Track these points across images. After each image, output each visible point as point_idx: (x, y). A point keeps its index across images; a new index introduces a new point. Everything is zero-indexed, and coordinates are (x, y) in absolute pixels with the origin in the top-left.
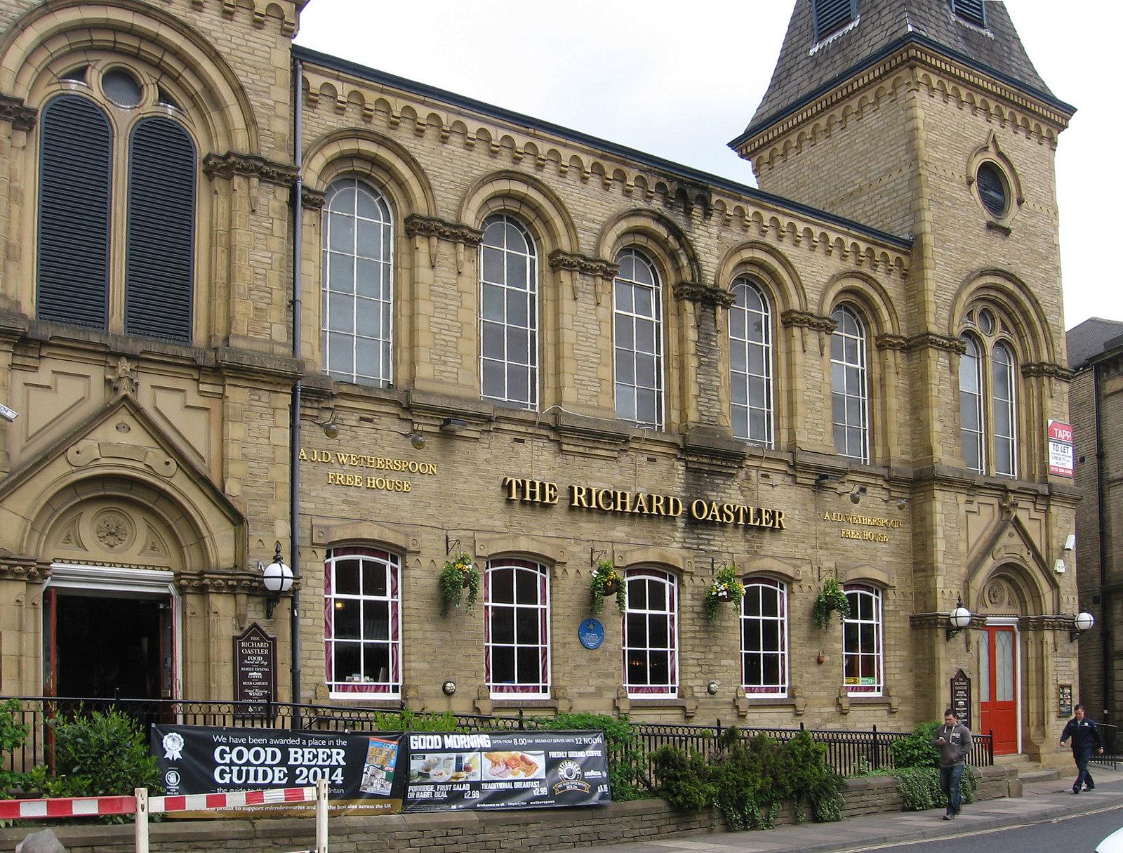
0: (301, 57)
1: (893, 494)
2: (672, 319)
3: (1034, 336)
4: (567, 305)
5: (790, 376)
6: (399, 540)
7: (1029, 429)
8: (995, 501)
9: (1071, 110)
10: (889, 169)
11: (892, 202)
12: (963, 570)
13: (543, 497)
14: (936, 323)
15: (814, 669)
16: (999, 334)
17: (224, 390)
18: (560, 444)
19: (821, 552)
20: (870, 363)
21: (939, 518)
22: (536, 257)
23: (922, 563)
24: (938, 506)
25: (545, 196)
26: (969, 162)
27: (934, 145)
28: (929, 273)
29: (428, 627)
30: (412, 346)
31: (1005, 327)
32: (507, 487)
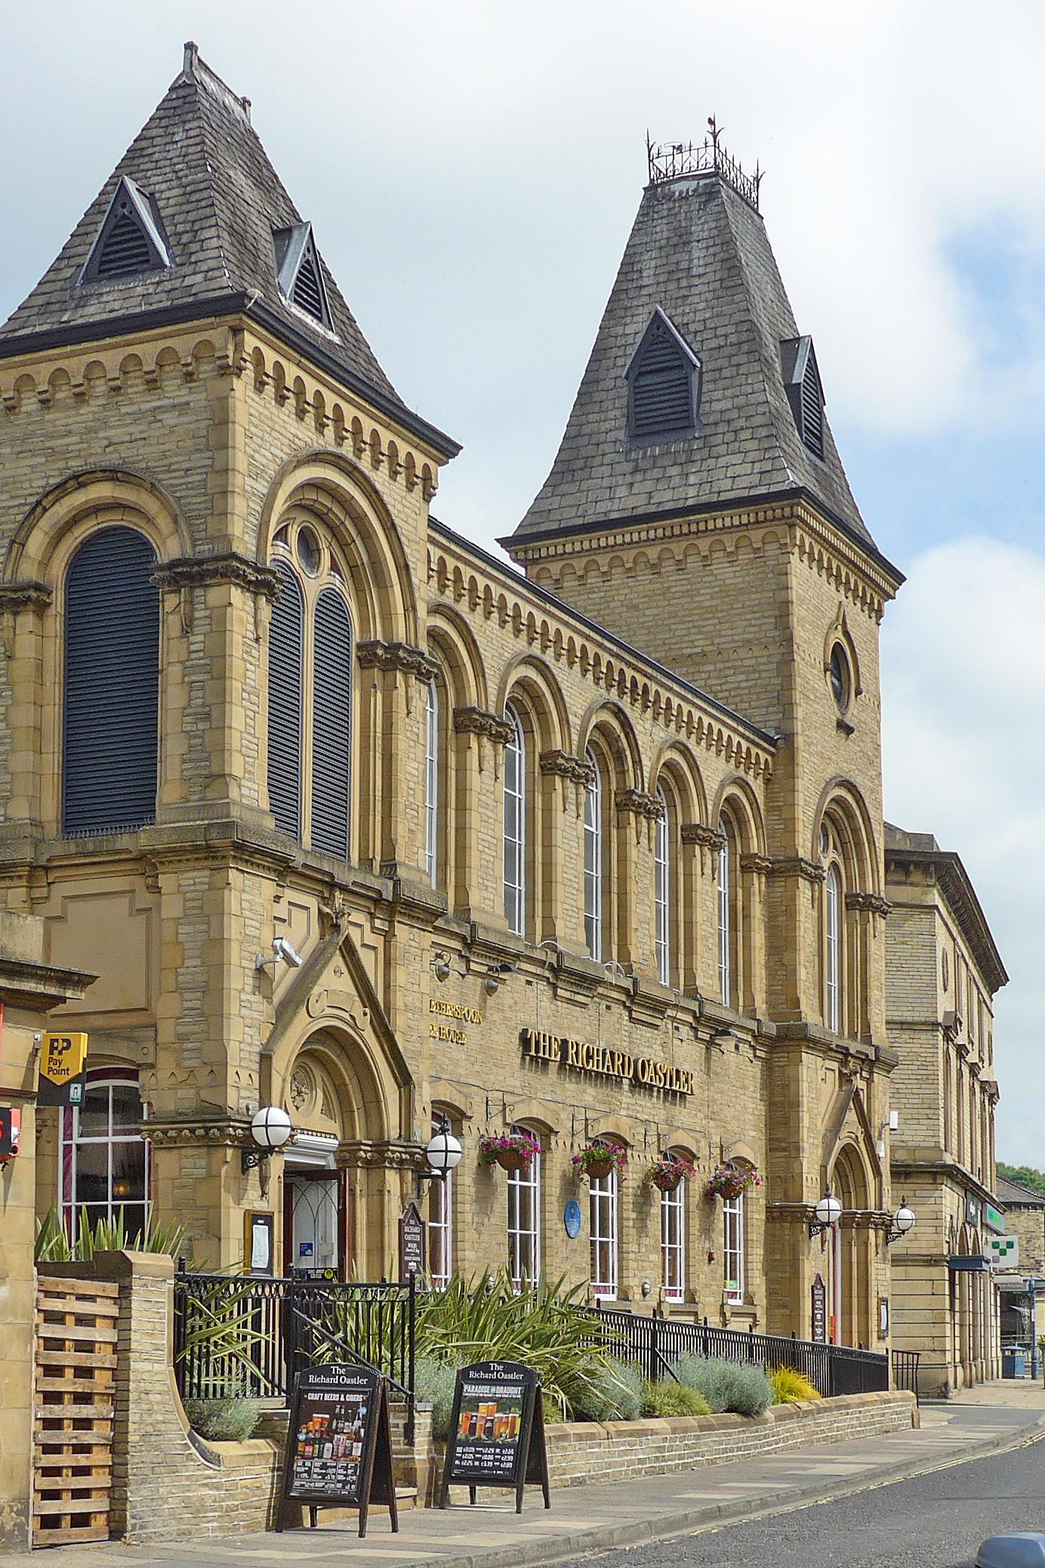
0: (433, 524)
1: (758, 1053)
2: (614, 832)
3: (861, 860)
8: (835, 1065)
9: (900, 578)
10: (749, 641)
11: (751, 683)
13: (537, 1051)
14: (804, 844)
18: (555, 987)
21: (804, 1087)
22: (523, 752)
25: (549, 685)
26: (826, 644)
31: (835, 848)
32: (525, 1041)
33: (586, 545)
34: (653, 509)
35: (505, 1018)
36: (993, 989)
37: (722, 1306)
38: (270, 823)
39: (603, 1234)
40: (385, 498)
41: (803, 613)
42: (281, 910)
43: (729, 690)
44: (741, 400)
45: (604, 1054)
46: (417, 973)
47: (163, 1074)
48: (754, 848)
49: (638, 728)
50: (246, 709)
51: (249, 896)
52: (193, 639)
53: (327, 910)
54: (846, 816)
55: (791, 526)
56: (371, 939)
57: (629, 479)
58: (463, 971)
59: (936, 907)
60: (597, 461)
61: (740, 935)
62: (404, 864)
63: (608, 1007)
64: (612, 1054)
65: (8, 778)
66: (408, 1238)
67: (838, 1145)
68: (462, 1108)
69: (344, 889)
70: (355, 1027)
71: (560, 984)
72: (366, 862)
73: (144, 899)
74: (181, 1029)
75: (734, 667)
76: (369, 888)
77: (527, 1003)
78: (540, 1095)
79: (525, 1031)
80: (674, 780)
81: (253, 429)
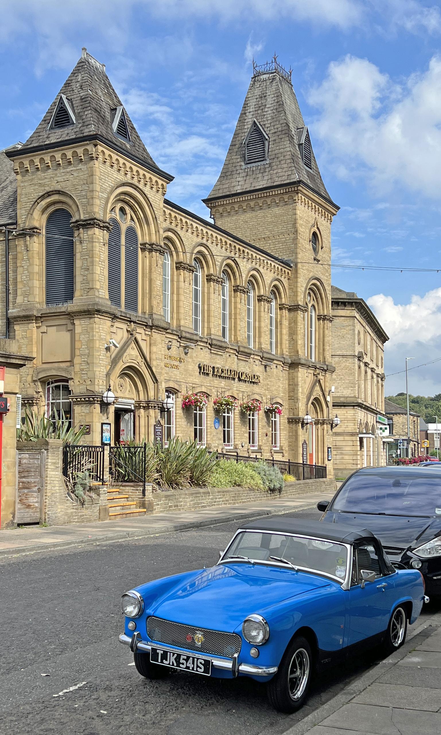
2: (233, 299)
4: (212, 296)
5: (260, 321)
6: (176, 387)
7: (319, 341)
8: (312, 372)
12: (306, 400)
13: (204, 370)
15: (265, 438)
16: (312, 302)
17: (152, 334)
19: (267, 392)
20: (276, 314)
21: (300, 379)
23: (293, 396)
24: (300, 375)
26: (310, 232)
27: (301, 225)
28: (299, 280)
29: (183, 420)
30: (178, 313)
31: (313, 300)
32: (200, 368)
33: (231, 202)
34: (252, 189)
35: (193, 360)
36: (384, 342)
37: (271, 450)
38: (109, 303)
39: (228, 427)
40: (148, 196)
41: (301, 222)
42: (114, 329)
43: (276, 249)
44: (282, 150)
45: (228, 370)
46: (159, 348)
47: (76, 381)
48: (283, 301)
49: (241, 264)
50: (100, 267)
51: (102, 326)
52: (83, 245)
53: (129, 329)
54: (315, 290)
55: (297, 193)
56: (144, 337)
57: (245, 178)
58: (178, 346)
59: (355, 317)
60: (235, 172)
61: (279, 330)
62: (155, 314)
63: (230, 356)
64: (230, 371)
65: (28, 288)
66: (157, 430)
67: (312, 398)
68: (178, 389)
69: (135, 322)
70: (139, 365)
71: (212, 349)
72: (144, 313)
73: (70, 327)
74: (82, 367)
75: (279, 241)
76: (143, 322)
77: (202, 355)
78: (205, 384)
79: (200, 364)
80: (253, 281)
81: (102, 177)
